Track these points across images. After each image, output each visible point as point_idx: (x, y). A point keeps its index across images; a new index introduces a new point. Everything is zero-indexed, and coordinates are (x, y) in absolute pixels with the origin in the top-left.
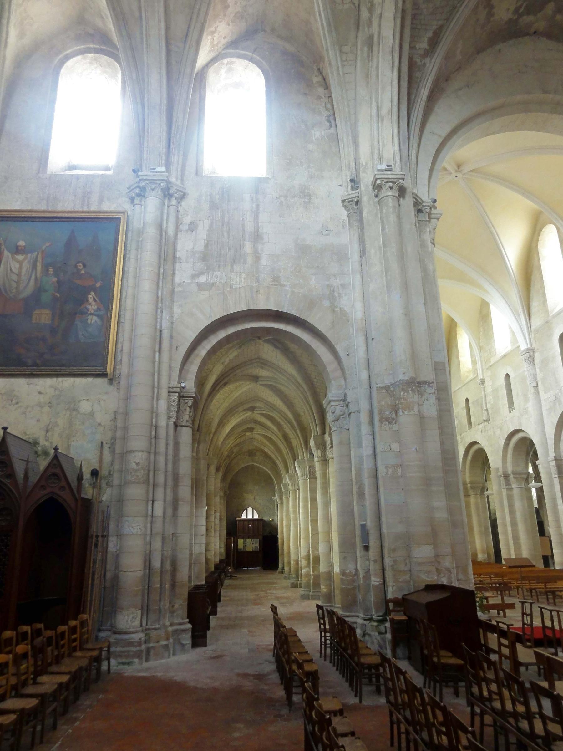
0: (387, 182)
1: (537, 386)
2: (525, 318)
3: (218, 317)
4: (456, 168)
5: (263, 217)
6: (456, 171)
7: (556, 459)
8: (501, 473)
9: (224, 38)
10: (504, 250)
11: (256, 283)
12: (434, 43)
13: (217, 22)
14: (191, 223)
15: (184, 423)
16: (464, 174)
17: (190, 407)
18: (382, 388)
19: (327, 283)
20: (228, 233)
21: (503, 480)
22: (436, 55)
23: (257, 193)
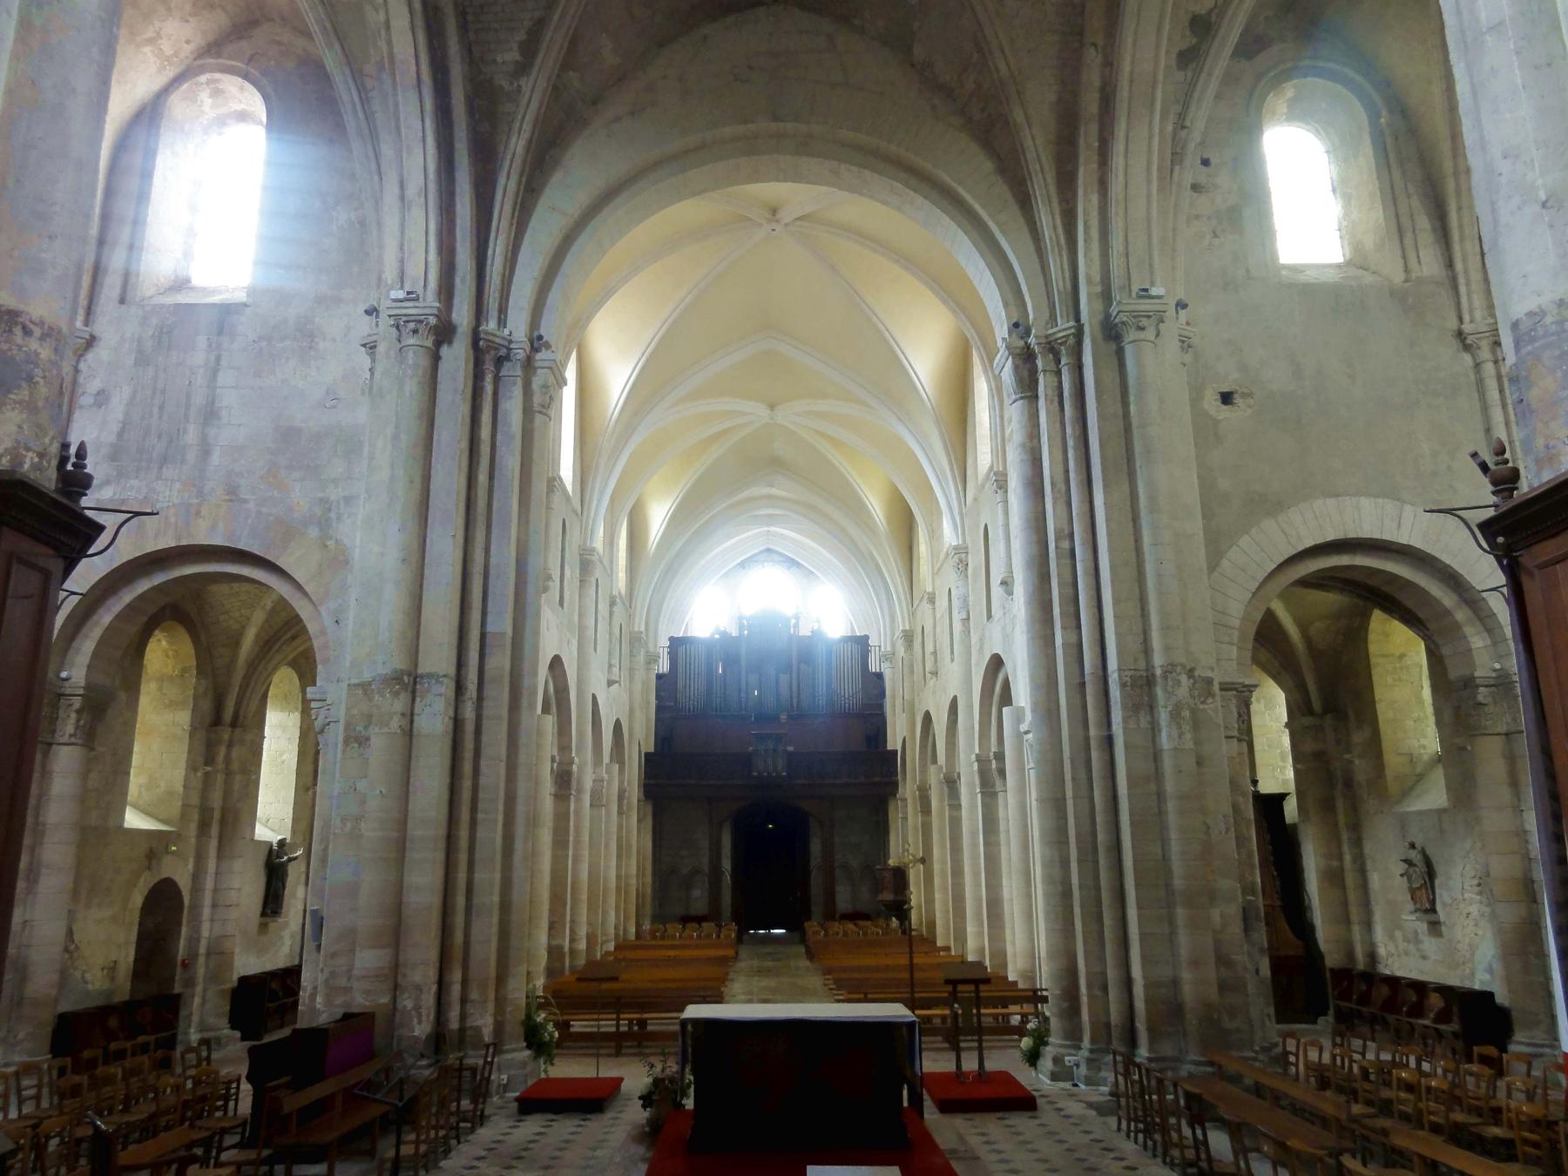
0: (408, 321)
1: (968, 619)
2: (956, 487)
3: (124, 560)
4: (770, 217)
5: (225, 378)
6: (769, 221)
7: (979, 759)
8: (942, 775)
9: (188, 42)
10: (906, 358)
11: (197, 498)
12: (529, 50)
13: (155, 22)
14: (99, 393)
15: (65, 739)
16: (786, 225)
17: (78, 712)
18: (359, 685)
19: (320, 495)
20: (161, 408)
21: (946, 789)
22: (536, 68)
23: (220, 332)
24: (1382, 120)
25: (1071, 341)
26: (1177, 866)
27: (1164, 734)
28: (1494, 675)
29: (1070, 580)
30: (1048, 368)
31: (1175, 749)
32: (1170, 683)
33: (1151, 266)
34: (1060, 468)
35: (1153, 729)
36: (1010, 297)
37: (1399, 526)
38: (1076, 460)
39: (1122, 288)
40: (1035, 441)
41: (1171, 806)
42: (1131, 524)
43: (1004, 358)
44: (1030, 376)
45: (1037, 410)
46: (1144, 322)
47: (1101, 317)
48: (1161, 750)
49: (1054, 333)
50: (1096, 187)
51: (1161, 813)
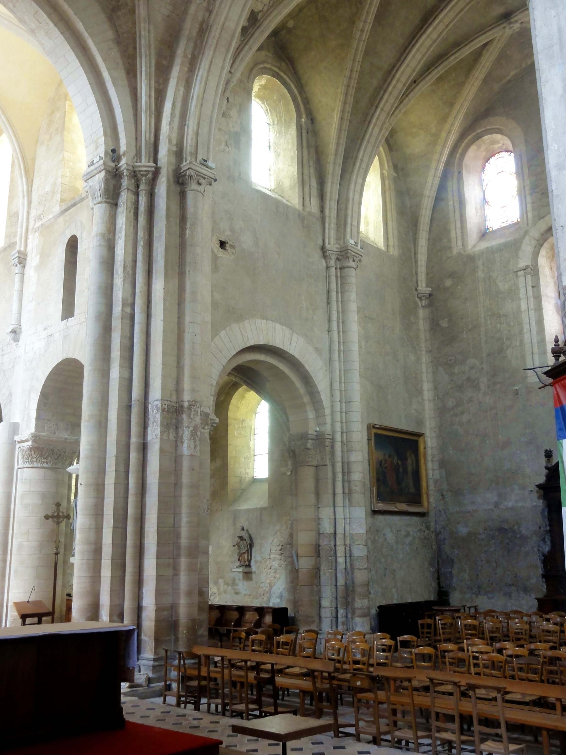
24: (303, 120)
25: (150, 176)
26: (184, 532)
27: (185, 445)
28: (315, 433)
29: (128, 335)
30: (130, 188)
31: (191, 455)
32: (193, 413)
33: (208, 148)
34: (130, 258)
35: (176, 441)
36: (109, 132)
37: (291, 344)
38: (143, 255)
39: (191, 154)
40: (111, 236)
41: (185, 492)
42: (177, 306)
43: (99, 169)
44: (114, 191)
45: (115, 214)
46: (202, 181)
47: (173, 167)
48: (182, 456)
49: (140, 166)
50: (184, 83)
51: (176, 497)
